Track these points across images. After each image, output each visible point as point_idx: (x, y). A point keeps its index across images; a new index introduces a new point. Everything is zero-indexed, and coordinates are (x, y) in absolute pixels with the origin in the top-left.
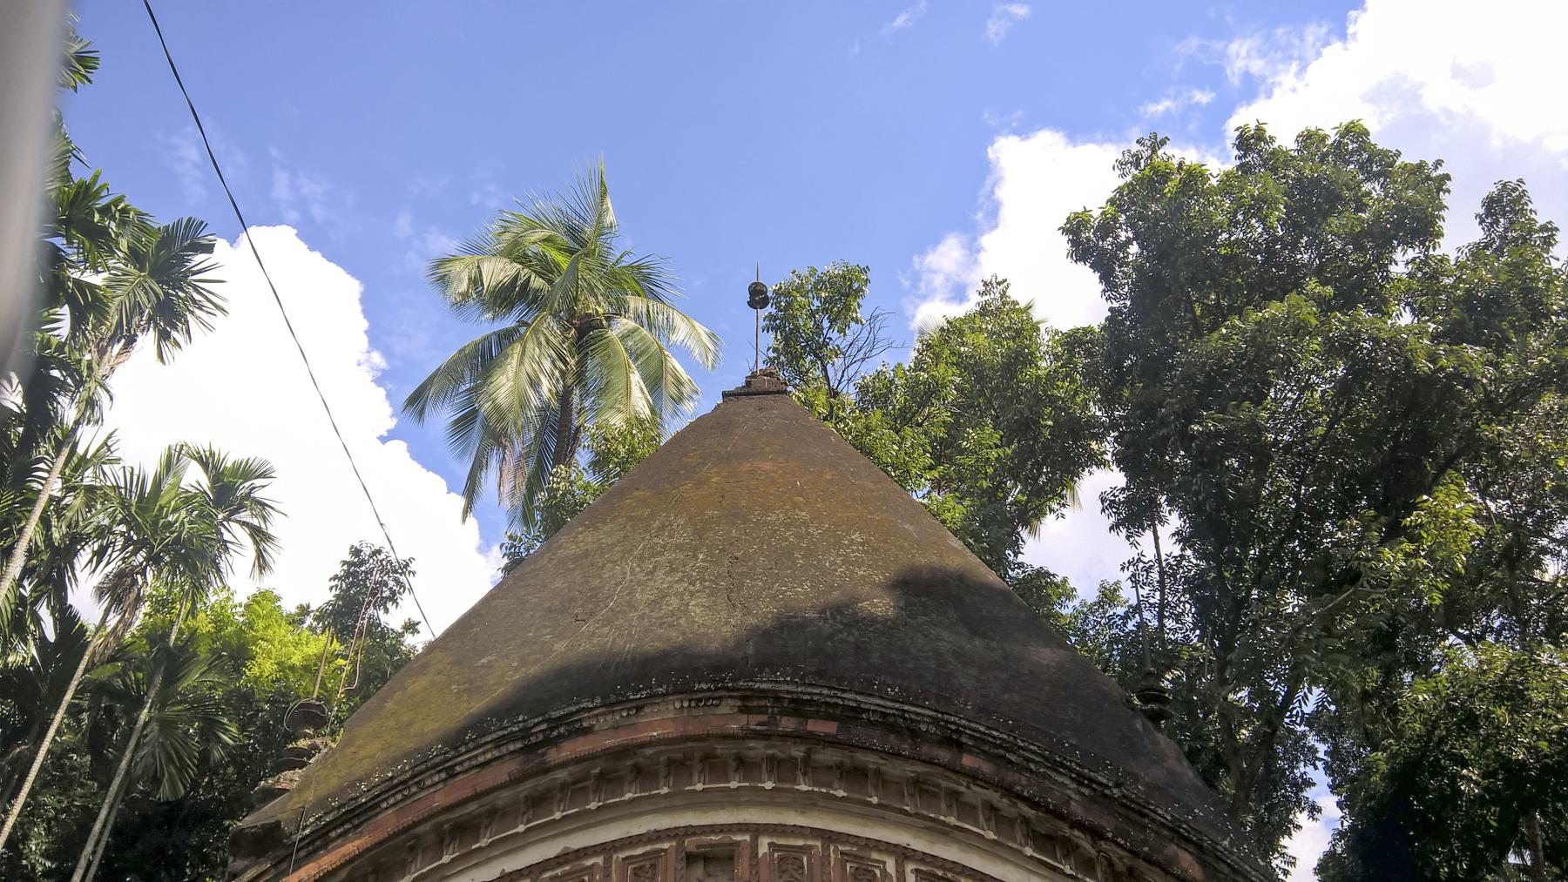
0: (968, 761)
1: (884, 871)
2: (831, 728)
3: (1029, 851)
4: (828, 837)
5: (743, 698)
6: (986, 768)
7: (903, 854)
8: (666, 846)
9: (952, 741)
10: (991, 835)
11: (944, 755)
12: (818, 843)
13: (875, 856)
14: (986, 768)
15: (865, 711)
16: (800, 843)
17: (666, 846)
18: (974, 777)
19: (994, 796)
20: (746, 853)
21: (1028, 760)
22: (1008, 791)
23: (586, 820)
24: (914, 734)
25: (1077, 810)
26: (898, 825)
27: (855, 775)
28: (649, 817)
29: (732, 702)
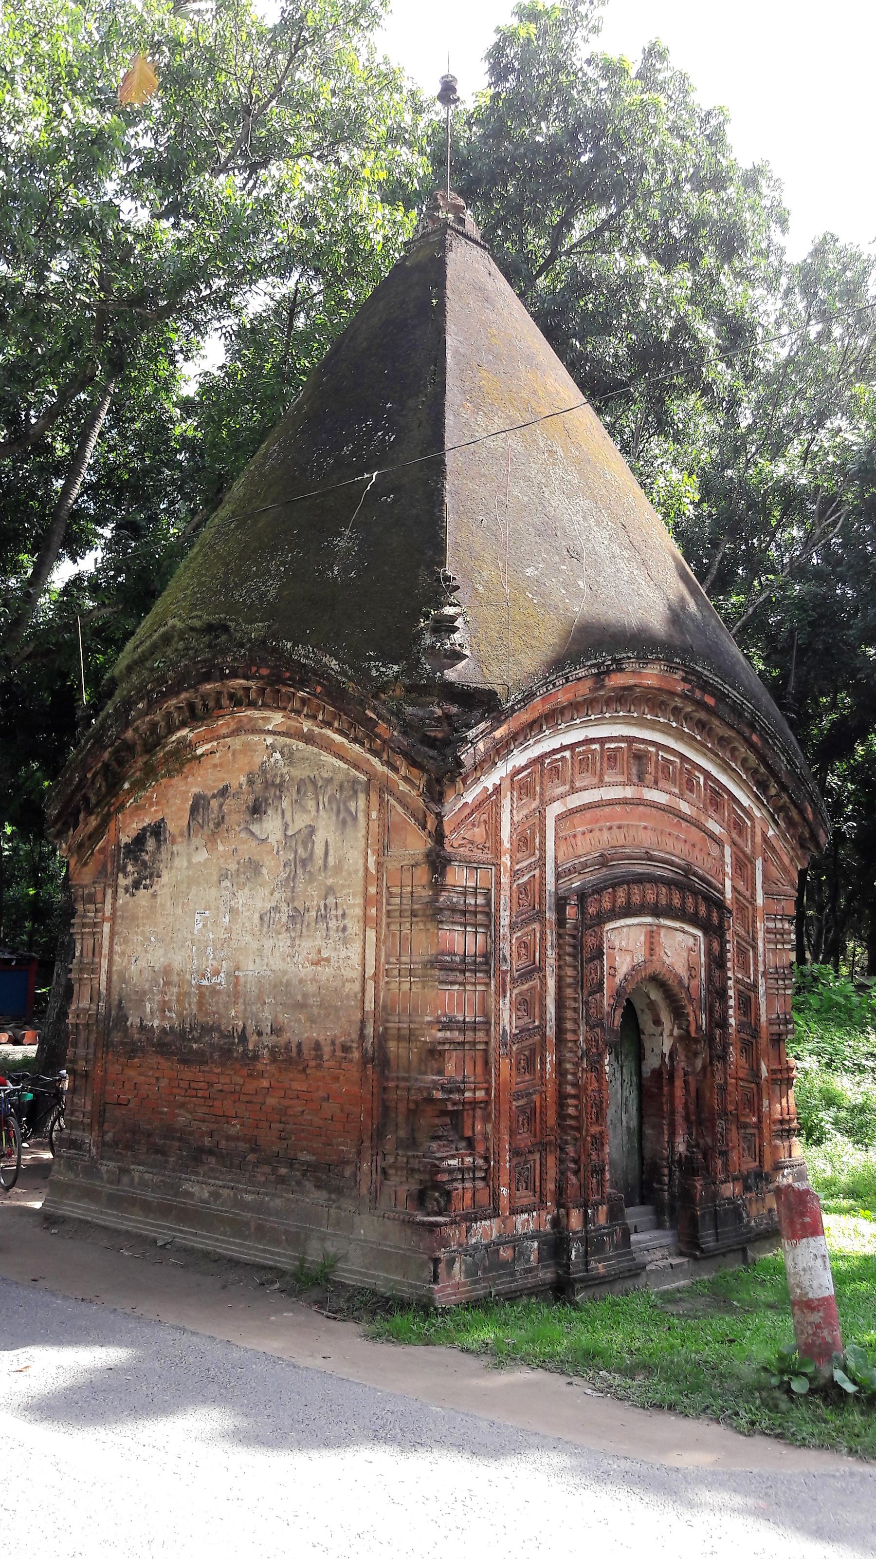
0: (755, 738)
1: (698, 783)
2: (710, 701)
3: (755, 789)
4: (684, 758)
5: (686, 672)
6: (759, 744)
7: (708, 775)
8: (623, 745)
9: (752, 726)
10: (744, 777)
11: (747, 732)
12: (678, 760)
13: (697, 774)
14: (759, 744)
15: (729, 697)
16: (672, 758)
17: (623, 745)
18: (751, 746)
19: (753, 758)
20: (654, 758)
21: (775, 744)
22: (763, 759)
23: (599, 722)
24: (740, 715)
25: (783, 774)
26: (711, 760)
27: (701, 725)
28: (619, 726)
29: (681, 673)
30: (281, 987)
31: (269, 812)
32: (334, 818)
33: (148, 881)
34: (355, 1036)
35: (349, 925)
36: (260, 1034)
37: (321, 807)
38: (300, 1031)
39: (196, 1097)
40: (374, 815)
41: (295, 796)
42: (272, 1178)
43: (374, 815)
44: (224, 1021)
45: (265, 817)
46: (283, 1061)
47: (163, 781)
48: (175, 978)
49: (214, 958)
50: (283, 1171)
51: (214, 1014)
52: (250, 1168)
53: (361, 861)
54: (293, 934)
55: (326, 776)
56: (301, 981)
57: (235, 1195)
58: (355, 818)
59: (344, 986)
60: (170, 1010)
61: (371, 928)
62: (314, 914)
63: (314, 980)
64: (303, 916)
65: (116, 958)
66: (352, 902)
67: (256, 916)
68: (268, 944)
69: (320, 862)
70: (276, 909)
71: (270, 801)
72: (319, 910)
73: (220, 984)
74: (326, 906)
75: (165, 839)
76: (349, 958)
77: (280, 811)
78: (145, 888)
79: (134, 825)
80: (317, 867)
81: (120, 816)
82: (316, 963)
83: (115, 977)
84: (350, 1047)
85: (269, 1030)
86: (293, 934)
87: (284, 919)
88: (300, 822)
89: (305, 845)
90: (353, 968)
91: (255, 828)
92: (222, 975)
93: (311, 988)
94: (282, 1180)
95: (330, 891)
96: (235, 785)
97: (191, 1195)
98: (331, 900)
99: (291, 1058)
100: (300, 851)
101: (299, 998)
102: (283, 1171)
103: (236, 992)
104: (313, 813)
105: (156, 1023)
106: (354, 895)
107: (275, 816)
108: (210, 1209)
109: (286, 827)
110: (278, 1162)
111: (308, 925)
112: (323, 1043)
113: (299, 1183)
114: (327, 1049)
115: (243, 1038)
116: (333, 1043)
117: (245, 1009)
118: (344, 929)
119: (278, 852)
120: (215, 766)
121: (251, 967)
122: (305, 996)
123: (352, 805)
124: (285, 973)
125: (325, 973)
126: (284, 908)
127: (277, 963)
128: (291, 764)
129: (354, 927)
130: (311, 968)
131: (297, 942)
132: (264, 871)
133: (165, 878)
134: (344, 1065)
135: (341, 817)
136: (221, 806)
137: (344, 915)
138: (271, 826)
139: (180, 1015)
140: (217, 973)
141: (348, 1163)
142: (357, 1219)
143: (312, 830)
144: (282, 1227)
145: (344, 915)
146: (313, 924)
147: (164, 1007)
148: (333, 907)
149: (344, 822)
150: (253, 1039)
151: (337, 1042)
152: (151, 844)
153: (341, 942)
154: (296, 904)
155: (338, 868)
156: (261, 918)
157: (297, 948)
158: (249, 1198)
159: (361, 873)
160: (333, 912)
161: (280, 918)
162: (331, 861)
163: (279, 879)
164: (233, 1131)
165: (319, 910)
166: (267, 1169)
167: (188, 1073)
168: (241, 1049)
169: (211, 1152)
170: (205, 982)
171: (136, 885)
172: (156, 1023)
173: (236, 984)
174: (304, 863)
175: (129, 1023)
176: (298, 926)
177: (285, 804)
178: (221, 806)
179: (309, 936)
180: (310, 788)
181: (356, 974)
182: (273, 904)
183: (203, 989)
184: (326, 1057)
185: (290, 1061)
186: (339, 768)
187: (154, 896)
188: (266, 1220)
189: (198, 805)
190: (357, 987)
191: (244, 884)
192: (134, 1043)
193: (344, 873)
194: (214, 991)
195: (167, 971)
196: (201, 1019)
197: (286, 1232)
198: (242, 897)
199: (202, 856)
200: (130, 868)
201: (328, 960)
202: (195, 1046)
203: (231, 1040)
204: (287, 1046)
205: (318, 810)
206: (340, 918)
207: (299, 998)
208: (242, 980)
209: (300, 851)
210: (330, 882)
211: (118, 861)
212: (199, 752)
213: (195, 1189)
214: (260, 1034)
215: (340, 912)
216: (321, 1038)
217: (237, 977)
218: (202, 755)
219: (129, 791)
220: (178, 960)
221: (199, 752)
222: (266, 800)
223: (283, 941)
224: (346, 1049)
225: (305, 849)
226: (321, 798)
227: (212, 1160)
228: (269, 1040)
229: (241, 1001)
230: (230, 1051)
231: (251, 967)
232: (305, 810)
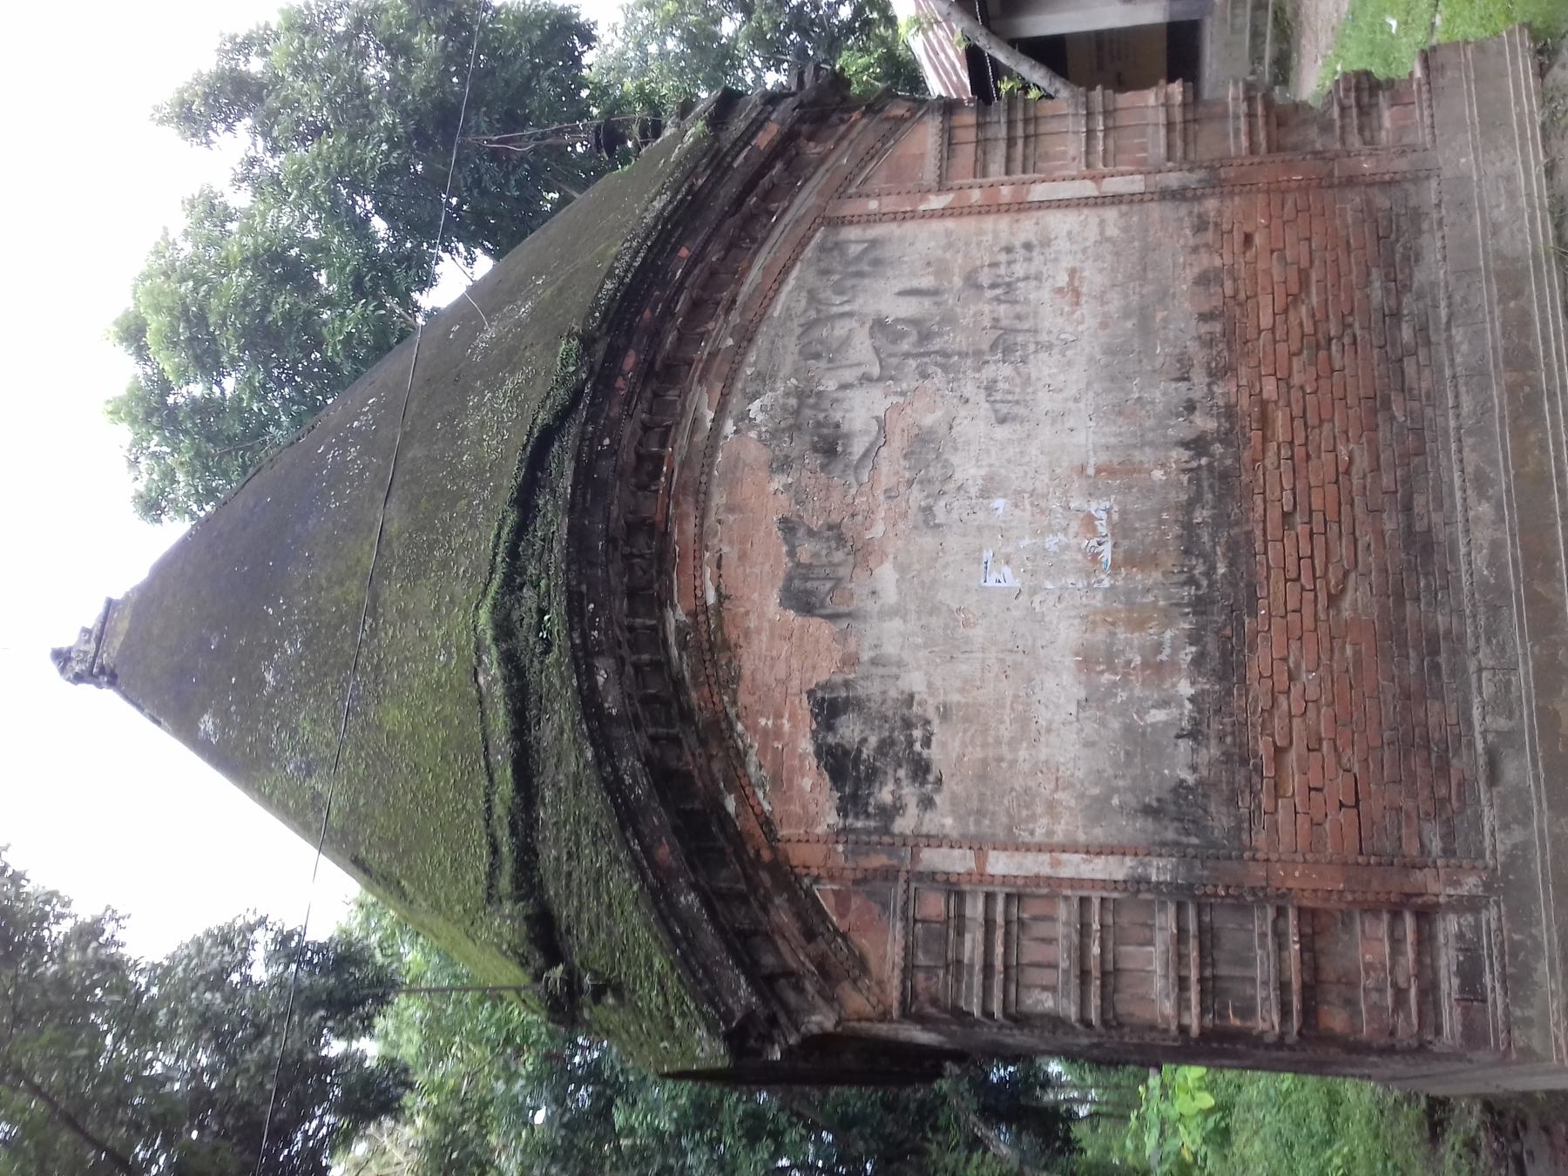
30: (1117, 364)
31: (837, 416)
32: (866, 281)
33: (917, 733)
34: (1183, 209)
35: (1022, 237)
36: (1191, 407)
37: (847, 308)
38: (1181, 323)
39: (1312, 557)
40: (873, 205)
41: (823, 364)
42: (1422, 353)
43: (873, 205)
44: (1172, 496)
45: (845, 428)
46: (1230, 350)
47: (743, 698)
48: (1101, 635)
49: (1065, 530)
50: (1406, 333)
51: (1161, 522)
52: (1416, 405)
53: (937, 226)
54: (1032, 347)
55: (803, 303)
56: (1104, 325)
57: (1470, 433)
58: (874, 243)
59: (1108, 239)
60: (1158, 647)
61: (1028, 192)
62: (1002, 308)
63: (1102, 299)
64: (1007, 331)
65: (1059, 837)
66: (990, 237)
67: (1001, 432)
68: (1045, 402)
69: (927, 302)
70: (990, 388)
71: (821, 416)
72: (998, 300)
73: (1108, 511)
74: (993, 286)
75: (847, 684)
76: (1069, 233)
77: (840, 394)
78: (927, 742)
79: (807, 783)
80: (934, 310)
81: (783, 832)
82: (1077, 294)
83: (1099, 834)
84: (1200, 216)
85: (1183, 385)
86: (1032, 347)
87: (1007, 370)
88: (862, 348)
89: (899, 337)
90: (1084, 224)
91: (858, 448)
92: (1093, 507)
93: (1115, 303)
94: (1422, 330)
95: (971, 282)
96: (783, 504)
97: (1496, 547)
98: (985, 278)
99: (1228, 332)
100: (905, 346)
101: (1129, 324)
102: (1406, 333)
103: (1116, 472)
104: (854, 324)
105: (1185, 688)
106: (981, 232)
107: (846, 405)
108: (1508, 491)
109: (866, 379)
110: (1393, 345)
111: (1019, 317)
112: (1196, 270)
113: (1420, 296)
114: (1206, 261)
115: (1197, 445)
116: (1195, 250)
117: (1151, 444)
118: (1028, 246)
119: (903, 394)
120: (743, 556)
121: (1080, 438)
122: (1126, 314)
123: (855, 250)
124: (1091, 360)
125: (1093, 278)
126: (988, 372)
127: (1075, 378)
128: (773, 377)
129: (1027, 228)
130: (1086, 308)
131: (1043, 337)
132: (928, 420)
133: (914, 681)
134: (1226, 227)
135: (866, 268)
136: (811, 533)
137: (1009, 250)
138: (860, 412)
139: (1167, 620)
140: (1089, 521)
141: (1369, 202)
142: (1447, 172)
143: (880, 325)
144: (1497, 312)
145: (1009, 250)
146: (1018, 308)
147: (1157, 669)
148: (994, 271)
149: (877, 263)
150: (1204, 423)
151: (1191, 242)
152: (850, 730)
153: (1047, 251)
154: (985, 347)
155: (941, 269)
156: (1002, 420)
157: (1052, 338)
158: (1467, 405)
159: (950, 223)
160: (1002, 270)
161: (1006, 379)
162: (927, 282)
163: (942, 385)
164: (1362, 462)
165: (998, 300)
166: (1410, 367)
167: (1275, 592)
168: (1218, 448)
169: (1408, 508)
170: (1106, 553)
171: (921, 769)
172: (1185, 688)
173: (1112, 472)
174: (925, 337)
175: (1190, 779)
176: (1020, 339)
177: (830, 385)
178: (811, 533)
179: (1036, 314)
180: (815, 333)
181: (1091, 216)
182: (983, 394)
183: (1120, 557)
184: (1218, 262)
185: (1229, 335)
186: (798, 278)
187: (945, 713)
188: (1494, 349)
189: (802, 600)
190: (1111, 214)
191: (947, 465)
192: (1228, 757)
193: (948, 255)
194: (1121, 529)
195: (1088, 660)
196: (1169, 560)
197: (1503, 300)
198: (968, 471)
199: (886, 575)
200: (885, 795)
201: (1072, 273)
202: (1221, 570)
203: (1204, 474)
204: (1208, 342)
205: (850, 315)
206: (1011, 257)
207: (1129, 324)
208: (1103, 458)
209: (905, 346)
210: (958, 281)
211: (868, 832)
212: (711, 598)
213: (1482, 535)
214: (1191, 407)
215: (1003, 257)
216: (1190, 274)
217: (1098, 471)
218: (718, 589)
219: (743, 800)
220: (1066, 633)
221: (711, 598)
222: (819, 425)
223: (1044, 367)
224: (1201, 226)
225: (903, 335)
226: (835, 310)
227: (1419, 501)
228: (1199, 377)
229: (1137, 456)
230: (1224, 476)
231: (1080, 438)
232: (846, 342)
